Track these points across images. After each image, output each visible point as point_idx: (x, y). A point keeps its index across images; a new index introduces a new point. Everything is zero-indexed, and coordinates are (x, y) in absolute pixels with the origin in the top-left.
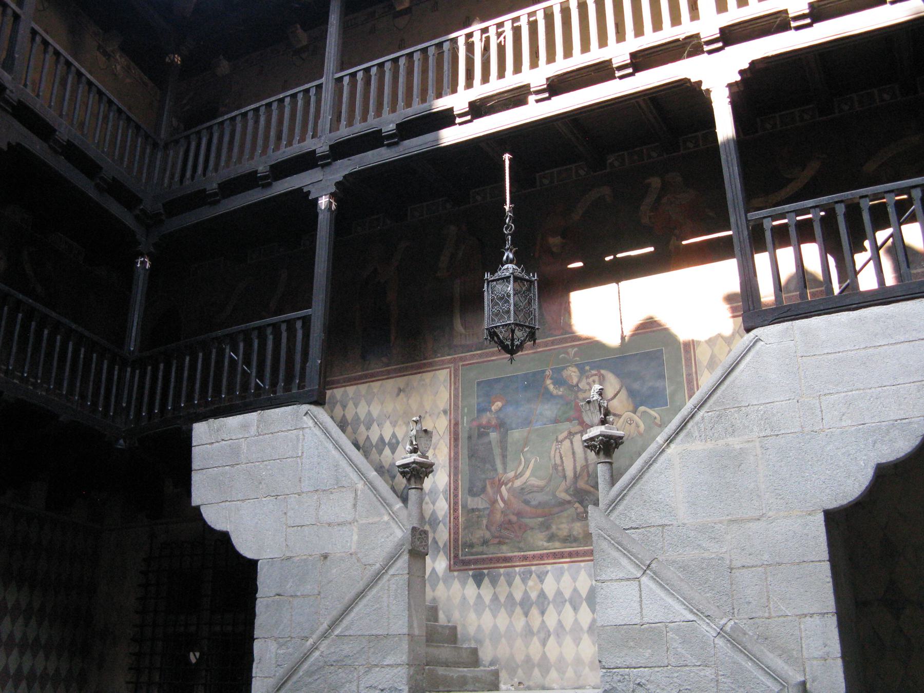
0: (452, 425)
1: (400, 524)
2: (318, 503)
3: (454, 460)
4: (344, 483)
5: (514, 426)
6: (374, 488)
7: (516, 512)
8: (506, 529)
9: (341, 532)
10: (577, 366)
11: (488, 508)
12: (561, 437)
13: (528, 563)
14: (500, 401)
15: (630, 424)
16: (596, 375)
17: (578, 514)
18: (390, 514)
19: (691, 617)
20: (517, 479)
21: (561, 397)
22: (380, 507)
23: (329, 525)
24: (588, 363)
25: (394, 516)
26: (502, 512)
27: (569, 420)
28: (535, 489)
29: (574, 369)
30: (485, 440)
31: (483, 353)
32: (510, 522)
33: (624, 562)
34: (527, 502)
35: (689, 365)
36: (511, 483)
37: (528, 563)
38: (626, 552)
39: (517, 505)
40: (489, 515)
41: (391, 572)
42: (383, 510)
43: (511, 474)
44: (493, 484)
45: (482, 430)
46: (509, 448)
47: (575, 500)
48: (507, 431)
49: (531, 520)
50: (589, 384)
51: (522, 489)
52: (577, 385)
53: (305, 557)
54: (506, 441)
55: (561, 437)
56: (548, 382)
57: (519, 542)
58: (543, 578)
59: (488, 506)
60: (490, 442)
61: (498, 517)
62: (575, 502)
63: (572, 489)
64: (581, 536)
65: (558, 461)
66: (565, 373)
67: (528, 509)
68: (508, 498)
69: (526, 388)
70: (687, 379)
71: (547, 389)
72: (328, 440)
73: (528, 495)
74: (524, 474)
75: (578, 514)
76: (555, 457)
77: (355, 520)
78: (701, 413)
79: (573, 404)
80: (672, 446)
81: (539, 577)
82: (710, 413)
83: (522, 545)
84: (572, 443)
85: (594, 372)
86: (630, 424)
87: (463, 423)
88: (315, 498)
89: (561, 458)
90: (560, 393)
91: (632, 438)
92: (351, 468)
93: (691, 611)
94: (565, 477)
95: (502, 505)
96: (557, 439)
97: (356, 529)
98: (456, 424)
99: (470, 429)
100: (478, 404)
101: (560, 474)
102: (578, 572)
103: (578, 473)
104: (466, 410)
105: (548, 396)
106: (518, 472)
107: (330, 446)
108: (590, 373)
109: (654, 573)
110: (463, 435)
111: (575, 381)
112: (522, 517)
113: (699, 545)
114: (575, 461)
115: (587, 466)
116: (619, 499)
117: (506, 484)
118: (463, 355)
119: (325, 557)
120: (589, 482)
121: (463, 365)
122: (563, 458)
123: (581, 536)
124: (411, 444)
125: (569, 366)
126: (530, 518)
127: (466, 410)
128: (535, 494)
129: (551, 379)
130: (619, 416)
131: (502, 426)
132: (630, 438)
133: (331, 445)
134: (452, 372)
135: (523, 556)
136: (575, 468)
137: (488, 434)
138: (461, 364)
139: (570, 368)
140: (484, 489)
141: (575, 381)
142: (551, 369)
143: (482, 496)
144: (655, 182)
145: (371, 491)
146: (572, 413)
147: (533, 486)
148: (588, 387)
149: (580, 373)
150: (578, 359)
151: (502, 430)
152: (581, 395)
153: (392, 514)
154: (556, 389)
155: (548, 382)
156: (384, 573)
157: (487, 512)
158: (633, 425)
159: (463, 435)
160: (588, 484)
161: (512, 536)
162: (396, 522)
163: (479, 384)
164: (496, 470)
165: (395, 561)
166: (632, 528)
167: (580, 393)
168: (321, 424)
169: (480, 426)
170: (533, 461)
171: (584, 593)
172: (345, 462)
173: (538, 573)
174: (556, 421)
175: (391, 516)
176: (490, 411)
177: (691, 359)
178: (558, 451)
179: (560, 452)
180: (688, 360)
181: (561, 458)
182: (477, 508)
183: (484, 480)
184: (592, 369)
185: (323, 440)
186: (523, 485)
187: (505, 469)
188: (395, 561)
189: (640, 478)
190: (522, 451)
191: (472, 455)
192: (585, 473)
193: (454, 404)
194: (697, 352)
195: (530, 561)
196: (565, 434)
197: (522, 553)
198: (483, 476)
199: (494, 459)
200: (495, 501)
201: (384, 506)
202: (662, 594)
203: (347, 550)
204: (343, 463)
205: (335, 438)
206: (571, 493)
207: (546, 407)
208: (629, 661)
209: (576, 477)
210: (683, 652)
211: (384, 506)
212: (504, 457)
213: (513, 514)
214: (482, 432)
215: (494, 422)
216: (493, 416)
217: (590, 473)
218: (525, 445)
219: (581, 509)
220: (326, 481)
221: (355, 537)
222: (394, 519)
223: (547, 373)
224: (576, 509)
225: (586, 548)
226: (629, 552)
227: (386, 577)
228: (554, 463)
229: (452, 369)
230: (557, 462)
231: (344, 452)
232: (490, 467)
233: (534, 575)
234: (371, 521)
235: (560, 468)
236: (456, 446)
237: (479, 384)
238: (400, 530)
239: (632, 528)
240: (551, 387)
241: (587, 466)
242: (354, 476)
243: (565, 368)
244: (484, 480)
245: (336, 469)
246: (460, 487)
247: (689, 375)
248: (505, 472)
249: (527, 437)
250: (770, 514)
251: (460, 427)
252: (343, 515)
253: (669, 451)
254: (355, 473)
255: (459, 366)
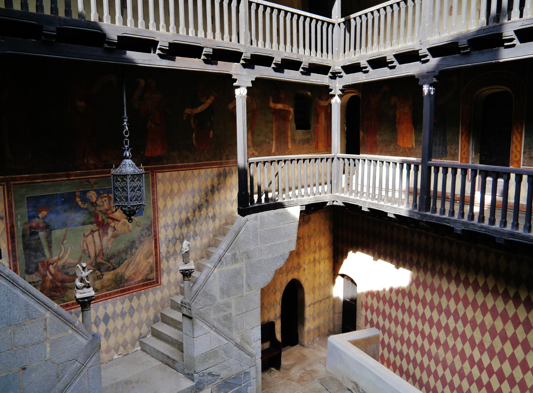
0: (9, 227)
1: (81, 333)
2: (12, 334)
3: (12, 252)
4: (34, 316)
5: (56, 227)
6: (58, 315)
7: (60, 280)
8: (54, 291)
9: (36, 349)
10: (95, 190)
11: (41, 280)
12: (86, 234)
13: (69, 308)
14: (45, 211)
15: (125, 225)
16: (106, 197)
17: (98, 277)
18: (73, 328)
19: (226, 342)
20: (60, 260)
21: (86, 209)
22: (64, 325)
23: (25, 346)
24: (102, 190)
25: (76, 330)
26: (51, 282)
27: (91, 223)
28: (71, 265)
29: (94, 192)
30: (36, 237)
31: (30, 176)
32: (57, 287)
33: (205, 327)
34: (67, 274)
35: (153, 194)
36: (56, 263)
37: (69, 308)
38: (205, 322)
39: (60, 276)
40: (41, 285)
41: (88, 365)
42: (67, 327)
43: (55, 258)
44: (43, 265)
45: (33, 230)
46: (53, 242)
47: (96, 269)
48: (51, 230)
49: (70, 283)
50: (102, 202)
51: (63, 266)
52: (96, 202)
53: (6, 374)
54: (51, 237)
55: (86, 234)
56: (78, 199)
57: (63, 297)
58: (79, 314)
59: (41, 279)
60: (39, 238)
61: (48, 284)
62: (96, 270)
63: (94, 263)
64: (99, 288)
65: (85, 248)
66: (88, 195)
67: (68, 277)
68: (55, 272)
69: (63, 203)
70: (152, 202)
71: (77, 203)
72: (16, 287)
73: (68, 270)
74: (64, 257)
75: (98, 277)
76: (83, 245)
77: (47, 338)
78: (226, 254)
79: (93, 214)
80: (216, 269)
81: (76, 314)
82: (230, 254)
83: (65, 299)
84: (93, 237)
85: (106, 195)
86: (125, 225)
87: (17, 226)
88: (9, 331)
89: (87, 246)
90: (85, 207)
91: (126, 233)
92: (38, 304)
93: (227, 339)
94: (89, 257)
95: (50, 277)
96: (84, 234)
97: (48, 345)
98: (12, 227)
99: (24, 230)
100: (29, 212)
101: (87, 255)
102: (98, 307)
103: (97, 254)
104: (19, 217)
105: (77, 208)
106: (61, 256)
107: (18, 292)
108: (103, 196)
109: (216, 328)
110: (18, 234)
111: (94, 201)
112: (65, 282)
113: (224, 310)
114: (95, 247)
115: (102, 250)
116: (195, 296)
117: (53, 264)
118: (14, 176)
119: (24, 369)
120: (104, 258)
121: (14, 184)
122: (88, 246)
123: (99, 288)
124: (82, 280)
125: (91, 190)
126: (70, 282)
127: (19, 217)
128: (71, 268)
129: (79, 198)
130: (119, 221)
131: (48, 228)
132: (125, 233)
133: (19, 290)
134: (6, 189)
135: (66, 305)
136: (95, 251)
137: (37, 233)
138: (12, 183)
139: (91, 191)
140: (37, 269)
141: (94, 200)
142: (80, 191)
143: (36, 273)
144: (142, 82)
145: (58, 317)
146: (93, 219)
147: (71, 264)
148: (102, 204)
149: (97, 195)
150: (96, 186)
151: (47, 230)
152: (98, 209)
153: (74, 328)
154: (83, 204)
155: (78, 199)
156: (83, 368)
157: (40, 283)
158: (126, 226)
159: (18, 234)
160: (103, 260)
161: (59, 294)
162: (78, 332)
163: (27, 198)
164: (45, 256)
165: (91, 358)
166: (200, 308)
167: (97, 207)
168: (7, 277)
169: (31, 228)
170: (69, 249)
171: (101, 317)
172: (33, 300)
173: (76, 312)
174: (84, 224)
175: (74, 329)
176: (39, 217)
177: (154, 192)
178: (85, 242)
179: (86, 242)
180: (153, 191)
181: (87, 246)
182: (32, 282)
183: (37, 263)
184: (104, 193)
185: (11, 288)
186: (63, 264)
187: (51, 254)
188: (91, 358)
189: (204, 285)
190: (63, 243)
191: (26, 247)
192: (101, 254)
193: (9, 212)
194: (158, 187)
195: (71, 307)
196: (89, 232)
197: (65, 303)
198: (36, 261)
199: (43, 249)
200: (46, 275)
201: (68, 324)
202: (217, 336)
203: (42, 359)
204: (32, 302)
205: (23, 286)
206: (94, 265)
207: (77, 215)
208: (206, 367)
209: (96, 256)
210: (224, 356)
211: (68, 324)
212: (50, 247)
213: (59, 282)
214: (34, 233)
215: (41, 225)
216: (41, 221)
217: (104, 253)
218: (64, 240)
219: (99, 274)
220: (18, 317)
221: (48, 349)
222: (76, 331)
223: (77, 194)
224: (97, 274)
225: (102, 294)
226: (206, 322)
227: (85, 371)
228: (83, 249)
229: (5, 186)
230: (85, 249)
231: (32, 295)
232: (41, 255)
233: (73, 314)
234: (60, 336)
235: (87, 252)
236: (13, 241)
237: (27, 198)
238: (80, 336)
239: (200, 308)
240: (80, 203)
241: (102, 250)
242: (42, 310)
243: (88, 191)
244: (37, 263)
245: (26, 307)
246: (19, 269)
247: (153, 200)
248: (51, 257)
249: (65, 235)
250: (246, 293)
251: (15, 228)
252: (36, 337)
253: (215, 271)
254: (43, 307)
255: (11, 185)
